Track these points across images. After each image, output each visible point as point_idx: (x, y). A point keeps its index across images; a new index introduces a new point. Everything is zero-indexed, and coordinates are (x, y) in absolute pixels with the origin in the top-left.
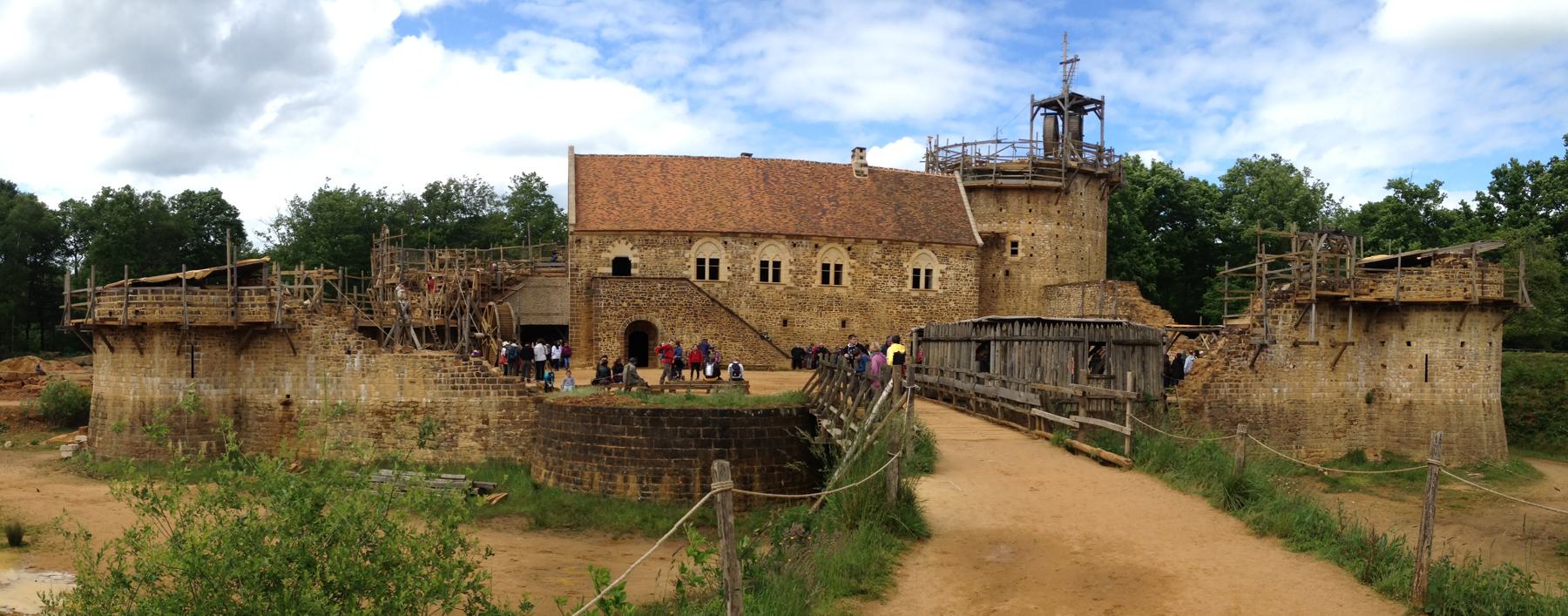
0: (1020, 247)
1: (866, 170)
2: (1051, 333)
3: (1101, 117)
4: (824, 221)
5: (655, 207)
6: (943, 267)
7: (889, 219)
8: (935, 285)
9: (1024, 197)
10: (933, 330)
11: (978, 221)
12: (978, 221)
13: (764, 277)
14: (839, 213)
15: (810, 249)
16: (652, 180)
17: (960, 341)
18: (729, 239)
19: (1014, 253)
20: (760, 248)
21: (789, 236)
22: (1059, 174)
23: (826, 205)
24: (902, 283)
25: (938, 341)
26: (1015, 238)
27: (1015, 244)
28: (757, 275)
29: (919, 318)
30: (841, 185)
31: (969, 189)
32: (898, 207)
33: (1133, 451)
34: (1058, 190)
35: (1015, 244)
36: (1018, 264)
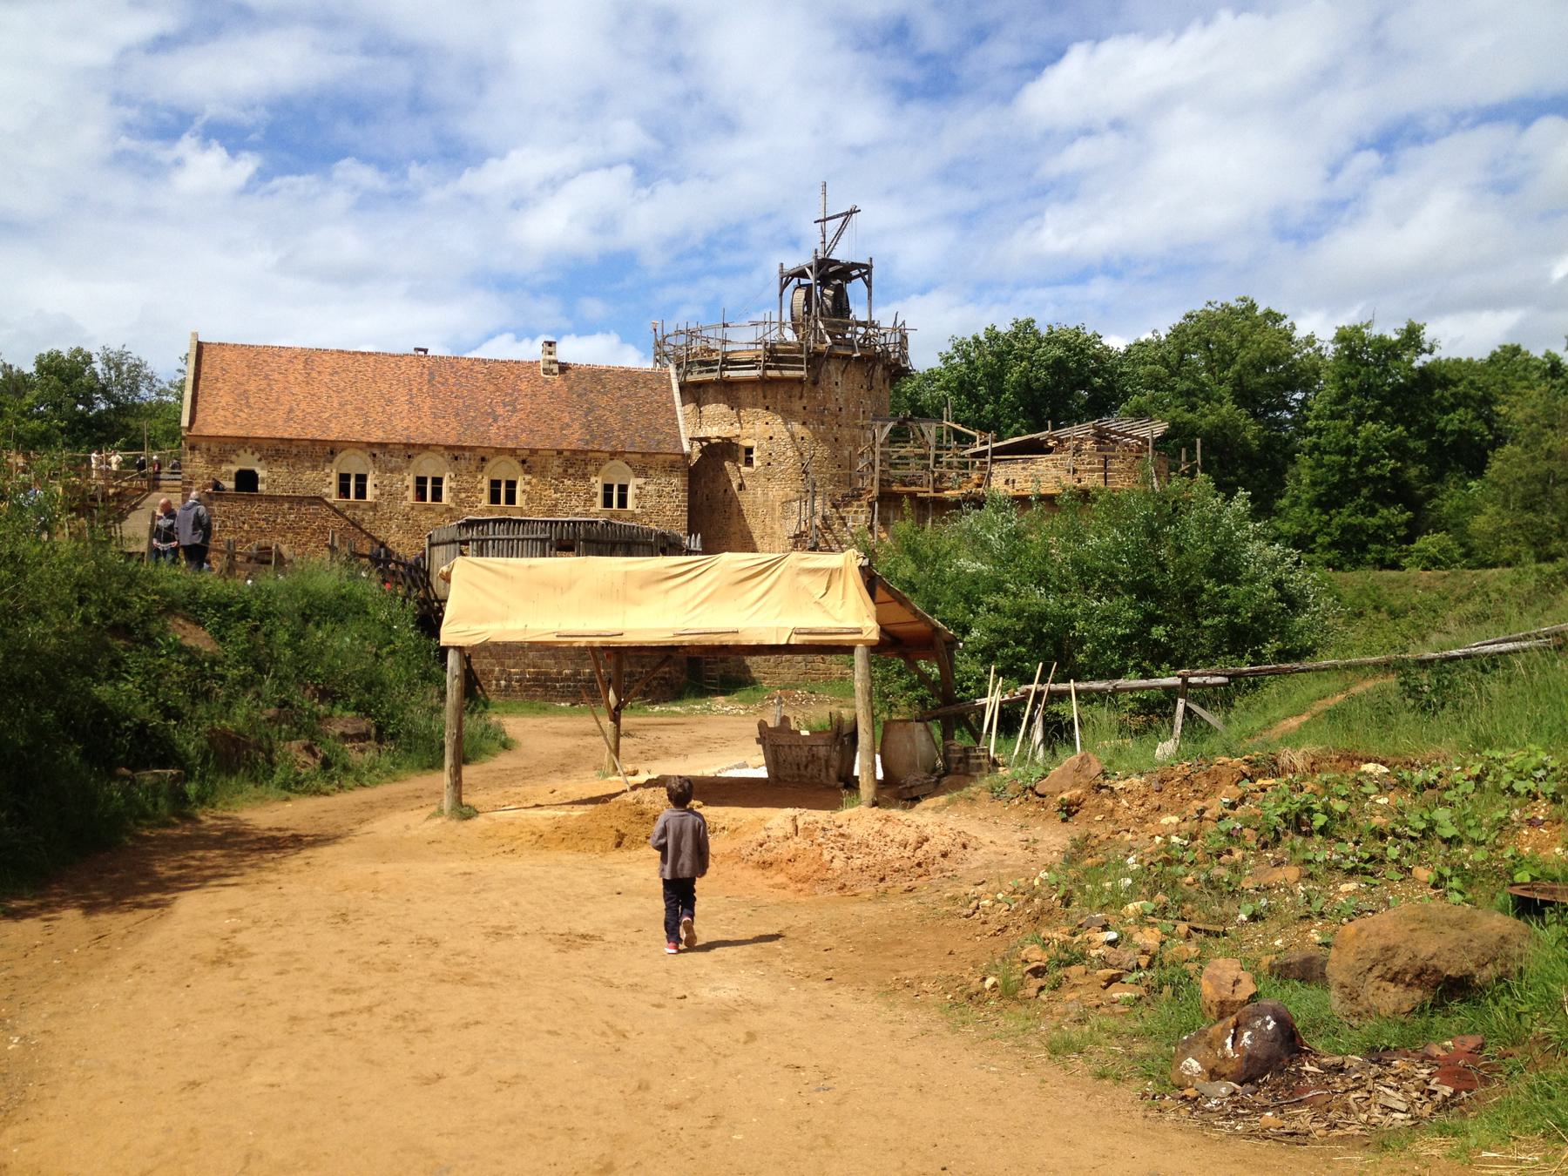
0: (755, 455)
1: (555, 368)
3: (868, 284)
4: (493, 430)
5: (291, 410)
6: (641, 481)
7: (576, 426)
8: (631, 504)
12: (717, 423)
13: (421, 495)
14: (515, 419)
16: (291, 379)
18: (376, 451)
19: (749, 462)
20: (415, 461)
21: (448, 448)
22: (801, 361)
23: (500, 411)
24: (590, 500)
26: (748, 443)
27: (749, 450)
28: (411, 494)
32: (590, 411)
34: (800, 380)
35: (749, 450)
36: (753, 476)
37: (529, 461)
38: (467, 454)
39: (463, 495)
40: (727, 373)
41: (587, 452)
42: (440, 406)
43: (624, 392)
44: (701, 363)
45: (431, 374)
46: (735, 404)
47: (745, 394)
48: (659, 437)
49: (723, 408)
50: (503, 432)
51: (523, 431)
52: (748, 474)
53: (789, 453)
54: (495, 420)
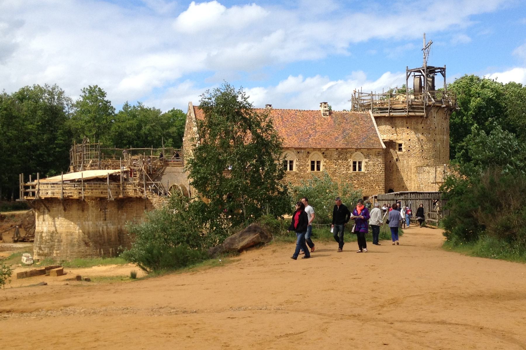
0: (403, 147)
2: (421, 197)
3: (444, 76)
6: (367, 160)
7: (340, 137)
8: (363, 170)
9: (405, 121)
10: (380, 196)
11: (384, 134)
15: (305, 154)
17: (391, 200)
19: (400, 149)
21: (295, 149)
22: (423, 109)
23: (311, 132)
24: (348, 169)
25: (383, 200)
26: (400, 142)
27: (400, 145)
29: (356, 186)
30: (317, 121)
31: (376, 118)
32: (344, 131)
33: (438, 225)
34: (422, 117)
35: (400, 145)
36: (402, 155)
37: (325, 152)
38: (303, 151)
39: (301, 168)
40: (392, 114)
41: (346, 149)
42: (289, 131)
43: (355, 123)
44: (380, 109)
45: (282, 117)
46: (394, 126)
47: (398, 122)
48: (372, 142)
49: (389, 127)
50: (314, 141)
51: (321, 141)
52: (400, 155)
53: (417, 146)
54: (310, 136)
